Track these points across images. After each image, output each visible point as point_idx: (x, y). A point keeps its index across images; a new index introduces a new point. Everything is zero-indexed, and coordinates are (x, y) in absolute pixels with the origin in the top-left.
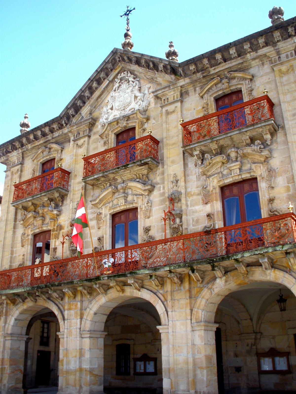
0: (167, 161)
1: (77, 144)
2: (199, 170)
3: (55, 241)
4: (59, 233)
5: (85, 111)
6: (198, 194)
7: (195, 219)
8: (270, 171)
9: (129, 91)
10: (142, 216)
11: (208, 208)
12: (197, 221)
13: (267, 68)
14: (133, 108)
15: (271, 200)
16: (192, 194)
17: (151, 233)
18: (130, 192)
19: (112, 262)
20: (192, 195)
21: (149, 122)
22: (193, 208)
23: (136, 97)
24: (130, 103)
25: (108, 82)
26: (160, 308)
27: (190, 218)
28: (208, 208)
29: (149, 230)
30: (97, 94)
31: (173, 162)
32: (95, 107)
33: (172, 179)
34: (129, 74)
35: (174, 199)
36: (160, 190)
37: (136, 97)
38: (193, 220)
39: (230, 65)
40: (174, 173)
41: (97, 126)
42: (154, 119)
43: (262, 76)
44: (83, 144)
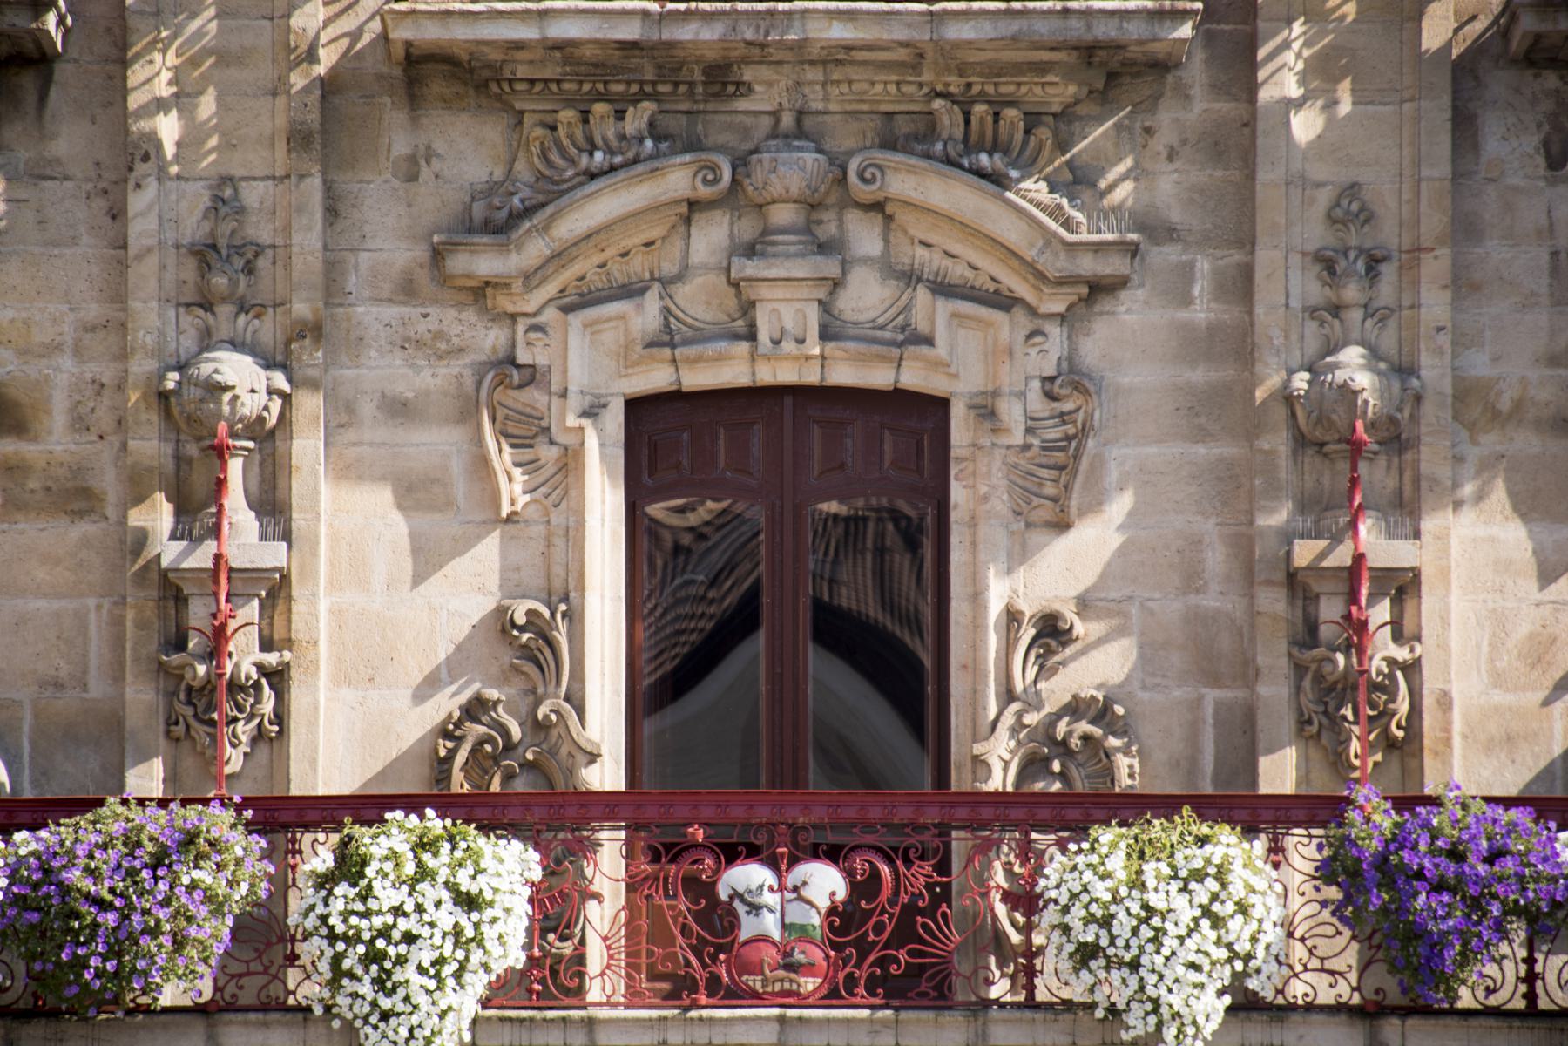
10: (1001, 503)
16: (1505, 404)
18: (865, 238)
19: (824, 904)
20: (1496, 417)
36: (1186, 301)
40: (1345, 176)
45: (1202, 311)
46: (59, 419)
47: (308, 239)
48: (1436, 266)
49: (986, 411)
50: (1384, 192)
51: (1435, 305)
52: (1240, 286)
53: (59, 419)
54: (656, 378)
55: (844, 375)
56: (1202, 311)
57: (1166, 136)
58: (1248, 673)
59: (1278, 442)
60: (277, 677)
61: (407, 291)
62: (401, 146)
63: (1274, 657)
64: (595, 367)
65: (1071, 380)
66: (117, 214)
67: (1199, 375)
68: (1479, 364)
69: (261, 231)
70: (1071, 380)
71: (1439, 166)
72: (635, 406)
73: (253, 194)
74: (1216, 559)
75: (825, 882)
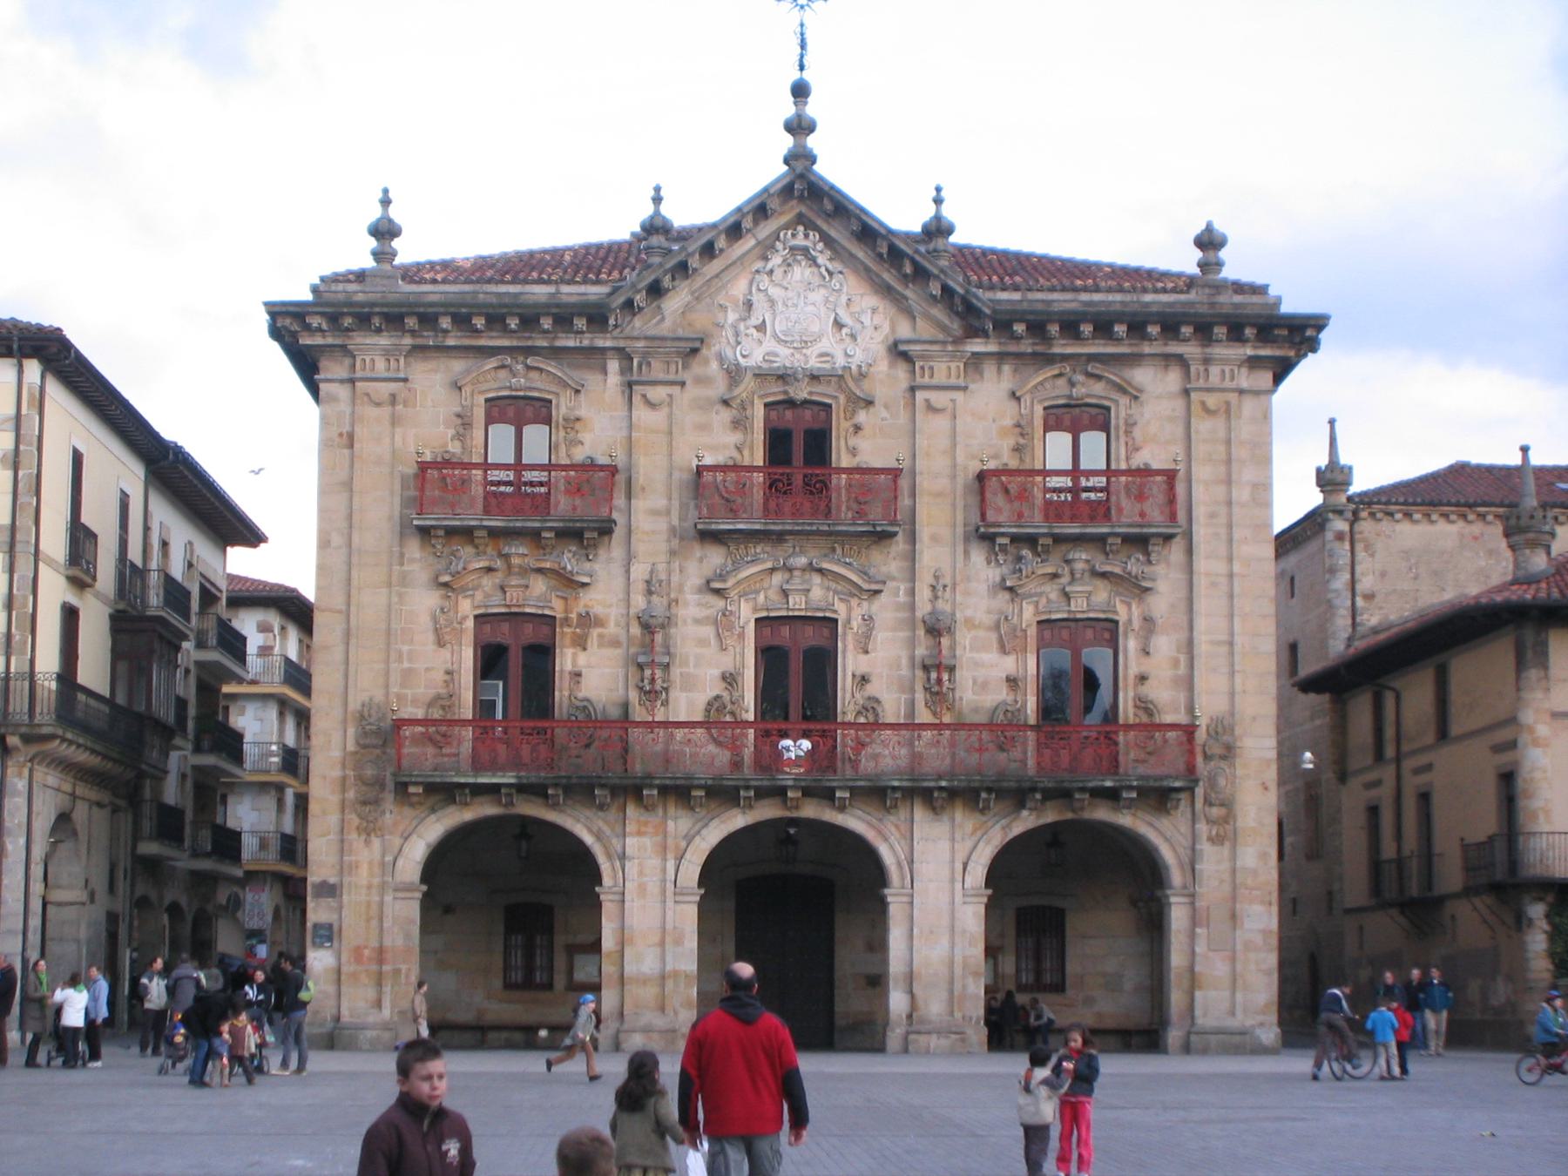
0: (924, 533)
1: (644, 396)
2: (993, 574)
5: (674, 303)
7: (980, 680)
8: (1148, 620)
11: (1009, 664)
12: (984, 686)
14: (827, 355)
15: (1142, 678)
17: (871, 689)
20: (974, 627)
21: (872, 410)
22: (976, 655)
23: (838, 325)
24: (820, 337)
25: (752, 242)
28: (1009, 664)
30: (716, 265)
34: (820, 246)
35: (935, 630)
37: (838, 325)
38: (975, 682)
41: (706, 362)
42: (886, 407)
43: (1159, 397)
45: (902, 598)
46: (612, 624)
49: (849, 621)
50: (946, 568)
52: (912, 592)
53: (612, 624)
54: (764, 614)
57: (893, 554)
58: (913, 690)
59: (921, 632)
60: (666, 689)
61: (700, 591)
62: (698, 554)
63: (919, 687)
64: (746, 614)
66: (628, 571)
68: (969, 613)
73: (661, 567)
74: (904, 662)
75: (806, 744)
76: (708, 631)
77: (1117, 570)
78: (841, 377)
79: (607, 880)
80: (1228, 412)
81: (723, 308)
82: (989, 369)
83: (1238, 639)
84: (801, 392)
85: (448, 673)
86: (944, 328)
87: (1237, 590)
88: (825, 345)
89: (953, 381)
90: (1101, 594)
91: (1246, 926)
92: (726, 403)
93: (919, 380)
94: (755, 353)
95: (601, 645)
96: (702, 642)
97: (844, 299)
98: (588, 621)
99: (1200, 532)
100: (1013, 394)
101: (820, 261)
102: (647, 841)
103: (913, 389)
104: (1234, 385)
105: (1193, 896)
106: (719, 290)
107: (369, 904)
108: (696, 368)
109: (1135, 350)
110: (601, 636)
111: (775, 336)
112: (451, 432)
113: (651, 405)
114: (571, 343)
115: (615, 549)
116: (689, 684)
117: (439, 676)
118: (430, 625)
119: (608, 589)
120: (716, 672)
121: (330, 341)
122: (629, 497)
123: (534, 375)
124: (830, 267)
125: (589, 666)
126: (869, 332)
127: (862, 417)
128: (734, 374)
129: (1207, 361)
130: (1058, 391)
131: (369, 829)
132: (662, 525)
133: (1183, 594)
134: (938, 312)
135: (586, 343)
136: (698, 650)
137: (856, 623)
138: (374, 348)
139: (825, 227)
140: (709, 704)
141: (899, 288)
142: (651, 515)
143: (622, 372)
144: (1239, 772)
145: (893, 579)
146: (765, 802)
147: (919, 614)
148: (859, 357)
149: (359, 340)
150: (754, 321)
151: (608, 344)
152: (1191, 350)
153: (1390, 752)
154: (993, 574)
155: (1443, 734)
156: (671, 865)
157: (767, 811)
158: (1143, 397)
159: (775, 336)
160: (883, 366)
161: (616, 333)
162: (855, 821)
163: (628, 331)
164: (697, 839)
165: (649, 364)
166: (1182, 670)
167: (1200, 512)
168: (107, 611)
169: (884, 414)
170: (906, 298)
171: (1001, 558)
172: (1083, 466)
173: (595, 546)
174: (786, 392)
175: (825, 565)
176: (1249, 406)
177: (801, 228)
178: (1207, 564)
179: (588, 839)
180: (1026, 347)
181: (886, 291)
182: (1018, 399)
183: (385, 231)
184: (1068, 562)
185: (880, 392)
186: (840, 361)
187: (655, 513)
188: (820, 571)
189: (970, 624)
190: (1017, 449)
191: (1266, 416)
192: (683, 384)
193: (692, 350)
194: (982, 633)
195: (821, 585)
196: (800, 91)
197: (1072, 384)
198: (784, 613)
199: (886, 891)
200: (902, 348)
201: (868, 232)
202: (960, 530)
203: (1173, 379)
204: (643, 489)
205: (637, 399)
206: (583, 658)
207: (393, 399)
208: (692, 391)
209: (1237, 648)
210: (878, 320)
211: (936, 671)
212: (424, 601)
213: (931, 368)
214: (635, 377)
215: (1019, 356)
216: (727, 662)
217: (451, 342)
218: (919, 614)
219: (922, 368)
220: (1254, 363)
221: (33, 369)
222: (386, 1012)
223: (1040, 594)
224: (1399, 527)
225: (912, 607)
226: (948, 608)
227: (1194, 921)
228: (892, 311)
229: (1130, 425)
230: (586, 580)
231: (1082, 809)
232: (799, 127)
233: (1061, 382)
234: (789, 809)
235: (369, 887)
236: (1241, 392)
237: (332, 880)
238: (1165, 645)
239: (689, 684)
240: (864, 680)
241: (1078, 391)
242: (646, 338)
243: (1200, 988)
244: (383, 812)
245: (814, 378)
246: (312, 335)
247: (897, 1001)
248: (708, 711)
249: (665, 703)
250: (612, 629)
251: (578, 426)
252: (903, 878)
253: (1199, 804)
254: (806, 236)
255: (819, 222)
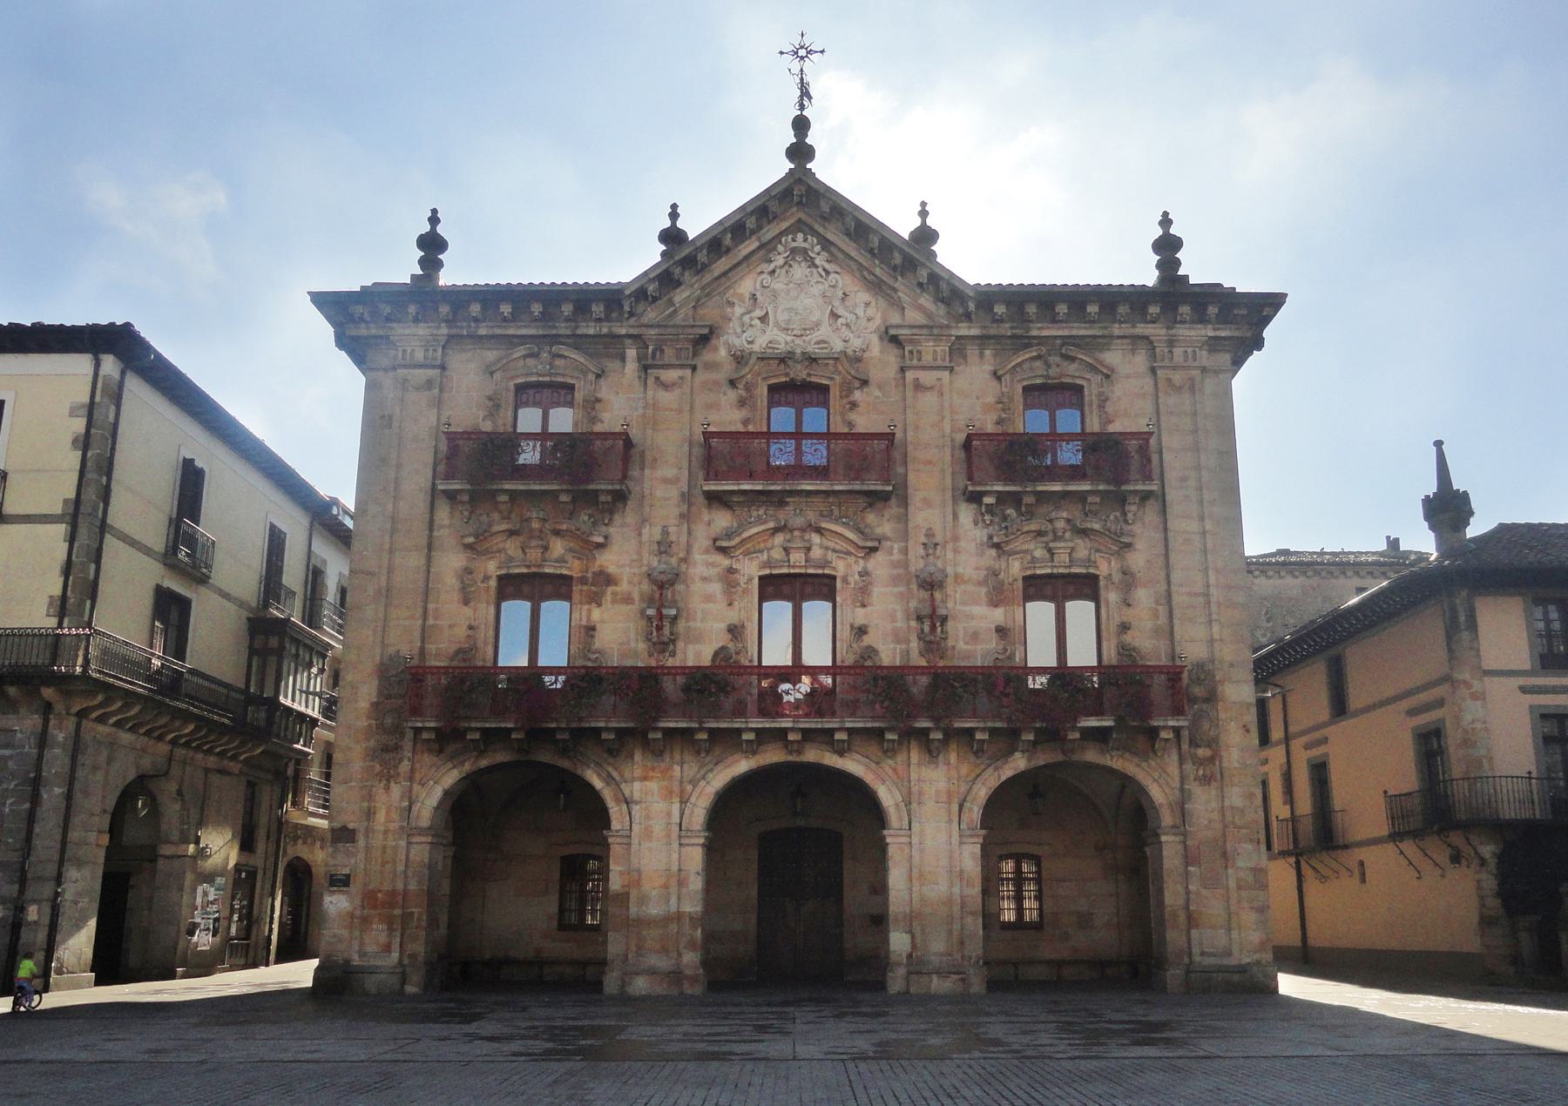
0: (916, 498)
1: (657, 379)
2: (980, 534)
3: (589, 611)
4: (603, 593)
6: (979, 584)
9: (816, 290)
12: (975, 637)
13: (1140, 360)
15: (1125, 627)
17: (867, 640)
20: (965, 582)
22: (967, 608)
23: (835, 316)
24: (818, 325)
25: (757, 244)
26: (887, 796)
27: (960, 626)
29: (865, 633)
30: (722, 265)
31: (927, 503)
32: (708, 295)
33: (923, 539)
35: (931, 584)
37: (835, 316)
39: (1074, 332)
41: (716, 349)
42: (880, 387)
43: (1128, 377)
44: (674, 384)
45: (896, 556)
47: (684, 539)
48: (950, 546)
49: (845, 580)
51: (950, 555)
52: (905, 551)
54: (767, 572)
55: (811, 571)
56: (896, 556)
58: (908, 642)
59: (914, 587)
60: (673, 641)
61: (707, 551)
65: (864, 573)
66: (640, 534)
67: (895, 572)
68: (960, 570)
69: (673, 538)
70: (864, 573)
71: (950, 525)
72: (761, 578)
74: (899, 615)
76: (716, 588)
77: (1097, 526)
78: (837, 359)
79: (615, 825)
80: (1192, 389)
81: (732, 304)
82: (972, 351)
83: (1213, 590)
84: (800, 373)
85: (471, 628)
86: (929, 316)
87: (1209, 545)
88: (824, 332)
89: (939, 362)
90: (1083, 548)
91: (1240, 863)
92: (733, 383)
93: (908, 363)
94: (762, 339)
95: (614, 602)
96: (709, 598)
97: (840, 294)
98: (606, 579)
99: (1172, 495)
100: (995, 373)
101: (817, 262)
102: (653, 786)
103: (903, 370)
104: (1196, 364)
105: (1184, 835)
106: (728, 288)
107: (384, 847)
108: (707, 356)
109: (1106, 332)
110: (614, 594)
111: (777, 324)
112: (481, 414)
113: (666, 386)
114: (591, 332)
115: (629, 516)
116: (699, 638)
117: (461, 632)
118: (457, 585)
119: (624, 554)
120: (723, 626)
121: (374, 331)
122: (643, 469)
123: (558, 362)
124: (827, 266)
125: (603, 621)
126: (863, 322)
127: (857, 395)
128: (740, 359)
129: (1171, 343)
130: (1037, 374)
131: (388, 777)
132: (674, 492)
133: (1160, 549)
134: (926, 301)
135: (605, 330)
136: (704, 606)
137: (854, 578)
138: (413, 337)
139: (821, 230)
140: (716, 654)
141: (890, 281)
142: (664, 481)
143: (639, 359)
144: (1222, 716)
145: (888, 539)
146: (770, 747)
147: (912, 569)
148: (856, 343)
149: (400, 331)
150: (758, 313)
151: (623, 331)
152: (1156, 331)
153: (1277, 733)
154: (980, 534)
155: (1340, 707)
156: (676, 808)
157: (772, 756)
158: (1114, 376)
159: (777, 324)
160: (876, 348)
161: (632, 321)
162: (853, 765)
163: (645, 320)
164: (702, 783)
165: (662, 351)
166: (1163, 620)
167: (1171, 476)
168: (245, 614)
169: (877, 393)
170: (895, 290)
171: (987, 518)
172: (1060, 430)
173: (612, 512)
174: (787, 375)
175: (824, 525)
176: (1210, 384)
177: (800, 236)
178: (1182, 524)
179: (598, 784)
180: (1006, 329)
181: (876, 286)
182: (999, 378)
183: (432, 245)
184: (1051, 521)
185: (875, 374)
186: (838, 346)
187: (666, 481)
188: (819, 531)
189: (958, 579)
190: (999, 422)
191: (1227, 395)
192: (694, 368)
193: (704, 341)
194: (970, 588)
195: (821, 546)
196: (801, 125)
197: (1048, 366)
198: (785, 571)
199: (885, 832)
200: (892, 332)
201: (861, 228)
202: (949, 494)
203: (1140, 360)
204: (655, 460)
205: (651, 381)
206: (596, 614)
207: (429, 384)
208: (701, 376)
209: (1213, 599)
210: (871, 311)
211: (932, 621)
212: (451, 562)
213: (919, 352)
214: (650, 362)
215: (998, 338)
216: (733, 616)
217: (482, 332)
218: (912, 569)
219: (911, 352)
220: (1214, 345)
221: (110, 365)
222: (395, 955)
223: (1026, 551)
224: (1257, 581)
225: (906, 565)
226: (939, 564)
227: (1189, 859)
228: (882, 303)
229: (1103, 400)
230: (600, 540)
231: (1072, 751)
232: (800, 152)
233: (1038, 364)
234: (791, 753)
235: (386, 832)
236: (1204, 370)
237: (351, 826)
238: (1143, 596)
239: (699, 638)
240: (861, 631)
241: (1053, 371)
242: (659, 326)
243: (1197, 926)
244: (401, 760)
245: (812, 360)
246: (356, 318)
247: (899, 942)
248: (713, 660)
249: (673, 654)
250: (624, 587)
251: (598, 406)
252: (901, 819)
253: (1185, 746)
254: (805, 240)
255: (817, 227)
